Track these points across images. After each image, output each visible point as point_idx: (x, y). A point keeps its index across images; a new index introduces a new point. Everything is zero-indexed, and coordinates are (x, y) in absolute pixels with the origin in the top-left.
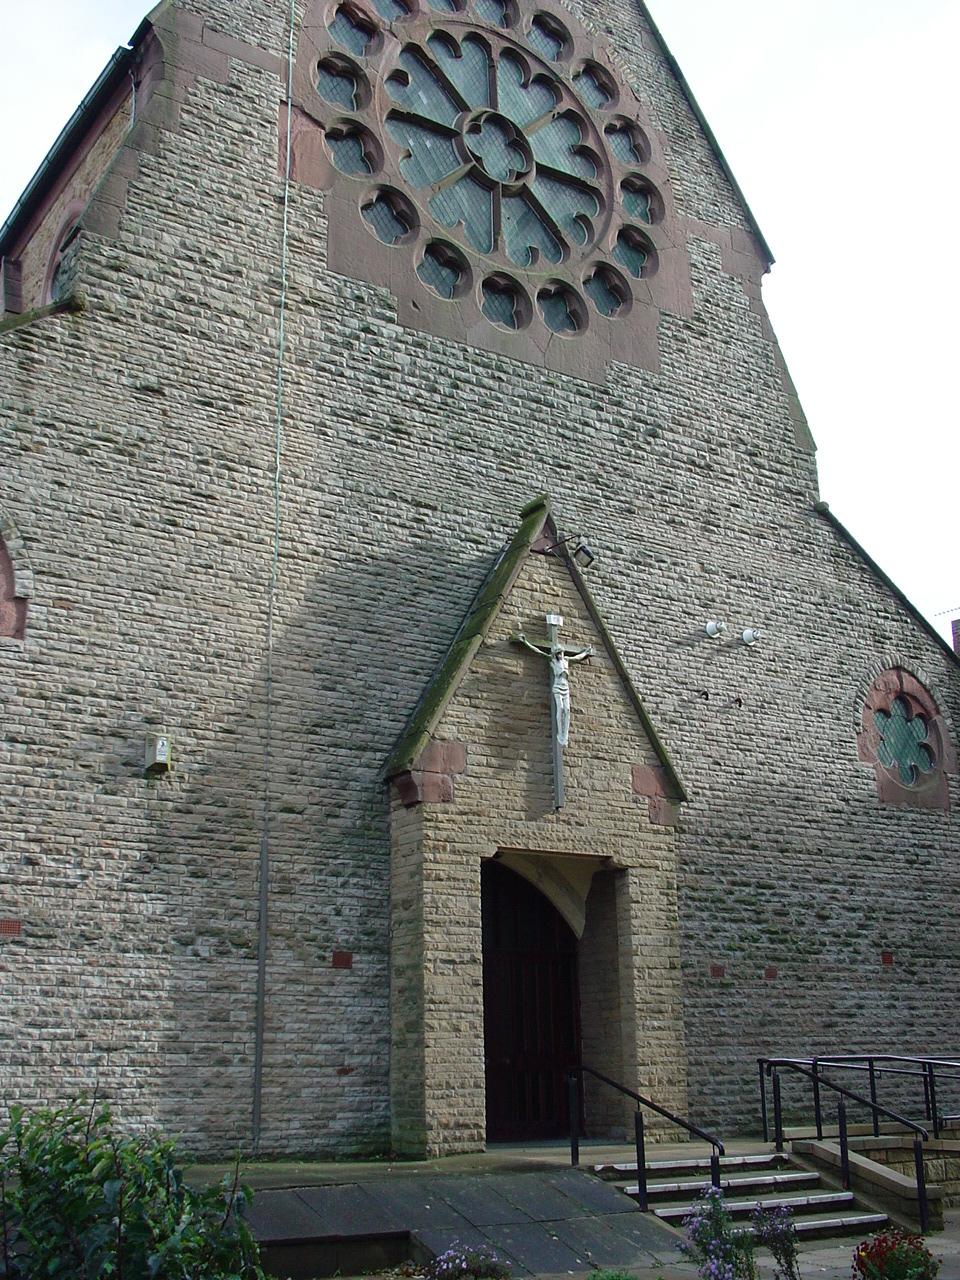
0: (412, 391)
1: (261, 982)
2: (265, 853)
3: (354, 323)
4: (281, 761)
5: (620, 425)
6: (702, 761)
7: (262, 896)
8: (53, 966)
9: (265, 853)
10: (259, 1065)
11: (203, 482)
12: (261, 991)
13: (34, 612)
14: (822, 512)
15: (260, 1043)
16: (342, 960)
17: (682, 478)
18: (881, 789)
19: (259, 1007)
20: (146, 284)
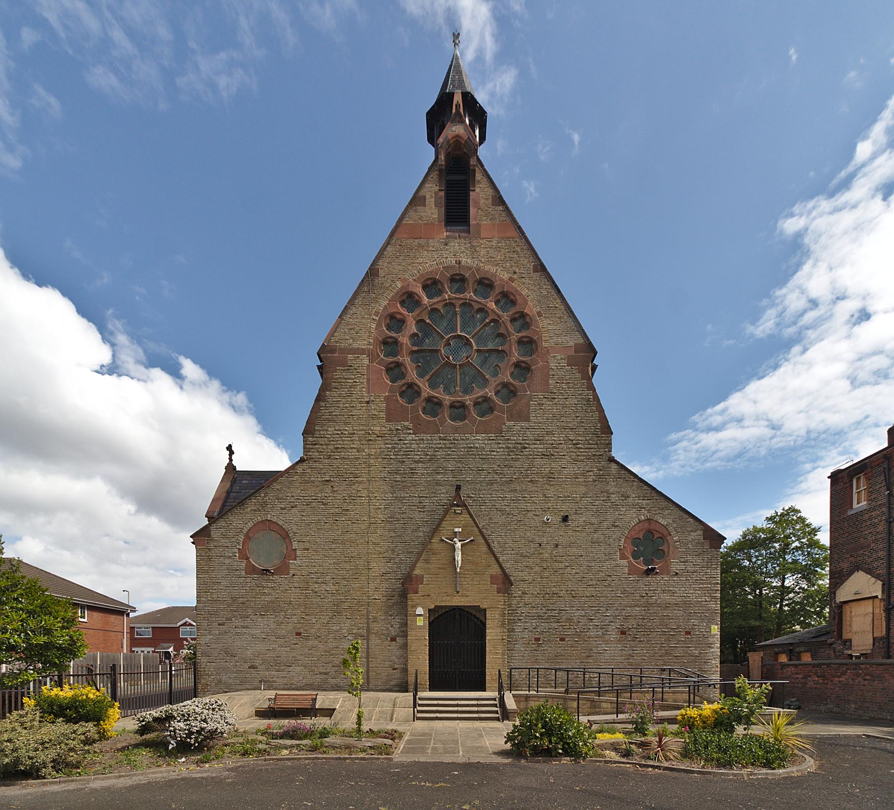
0: (418, 457)
1: (368, 646)
2: (368, 612)
3: (396, 438)
4: (372, 586)
5: (508, 448)
6: (537, 569)
7: (368, 623)
8: (310, 643)
9: (368, 612)
10: (368, 667)
11: (345, 507)
12: (368, 648)
13: (298, 553)
14: (612, 460)
15: (368, 662)
16: (393, 639)
17: (538, 462)
18: (629, 570)
19: (368, 652)
20: (324, 447)
